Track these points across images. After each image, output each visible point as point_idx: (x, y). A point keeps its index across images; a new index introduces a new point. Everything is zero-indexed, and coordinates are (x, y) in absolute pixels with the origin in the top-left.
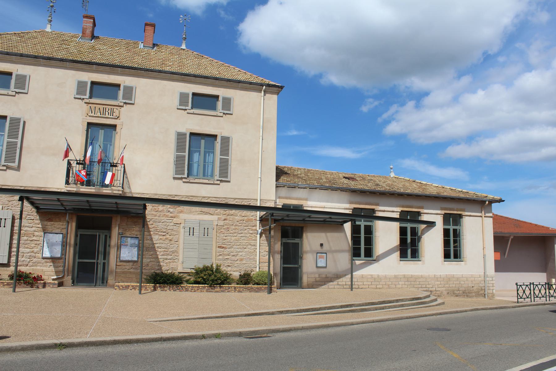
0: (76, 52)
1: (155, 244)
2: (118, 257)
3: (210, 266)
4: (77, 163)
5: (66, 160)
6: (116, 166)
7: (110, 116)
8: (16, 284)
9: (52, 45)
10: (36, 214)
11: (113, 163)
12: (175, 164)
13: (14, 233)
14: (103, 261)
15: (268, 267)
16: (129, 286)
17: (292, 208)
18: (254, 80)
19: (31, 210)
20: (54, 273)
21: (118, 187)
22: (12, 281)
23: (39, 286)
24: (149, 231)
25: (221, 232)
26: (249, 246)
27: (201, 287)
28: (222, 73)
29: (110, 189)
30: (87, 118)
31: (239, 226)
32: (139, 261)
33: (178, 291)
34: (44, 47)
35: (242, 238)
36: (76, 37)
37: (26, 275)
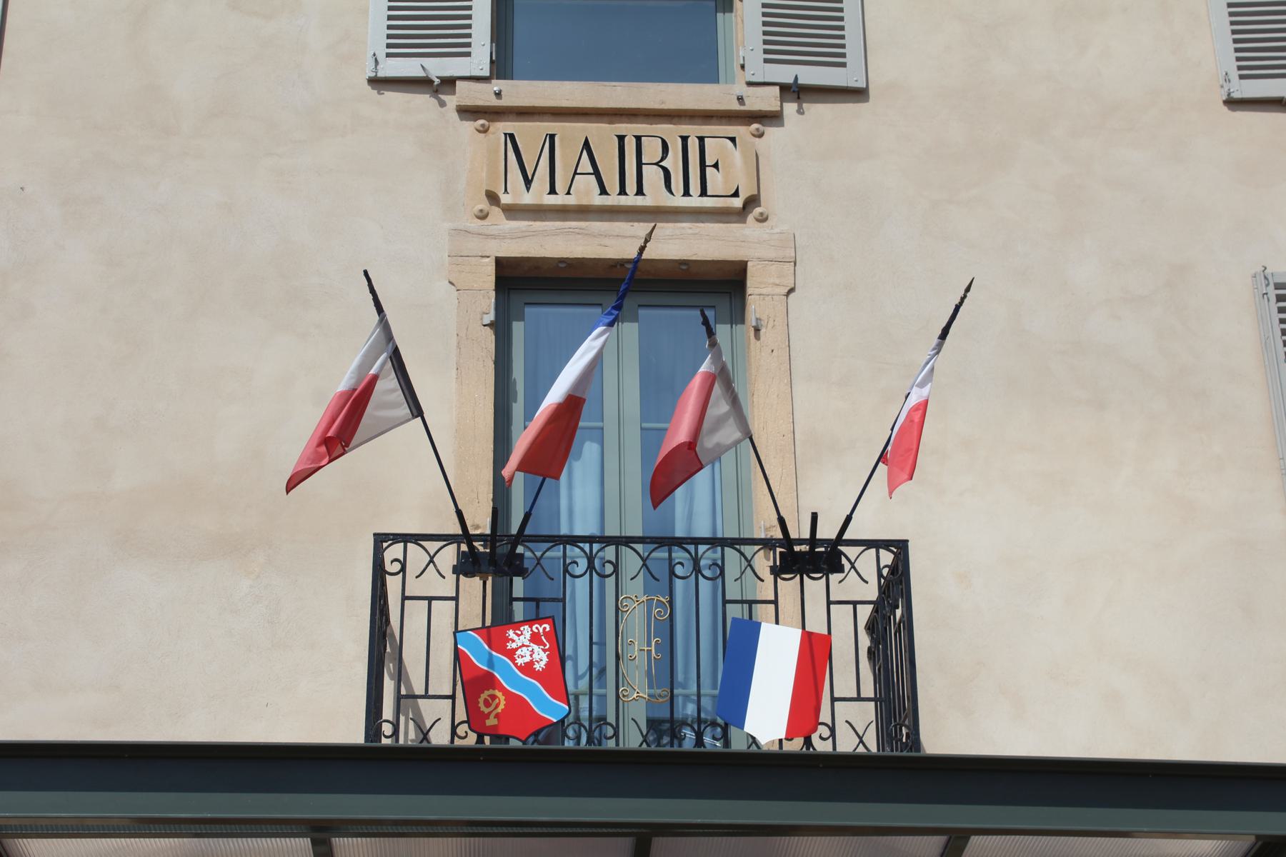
7: (679, 201)
30: (493, 230)
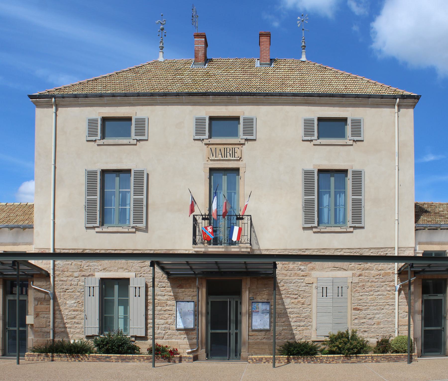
0: (191, 82)
1: (287, 308)
2: (250, 326)
3: (345, 332)
4: (203, 219)
5: (192, 216)
6: (242, 219)
8: (154, 358)
9: (167, 77)
10: (167, 280)
11: (239, 215)
12: (304, 210)
13: (149, 303)
14: (235, 331)
15: (407, 331)
16: (262, 358)
17: (433, 255)
18: (385, 92)
19: (162, 277)
20: (189, 345)
21: (245, 244)
22: (150, 356)
23: (175, 361)
24: (280, 294)
25: (357, 290)
26: (387, 306)
27: (336, 358)
28: (348, 87)
29: (238, 246)
31: (375, 282)
32: (272, 329)
33: (313, 362)
34: (158, 81)
35: (380, 297)
36: (189, 64)
37: (162, 349)
